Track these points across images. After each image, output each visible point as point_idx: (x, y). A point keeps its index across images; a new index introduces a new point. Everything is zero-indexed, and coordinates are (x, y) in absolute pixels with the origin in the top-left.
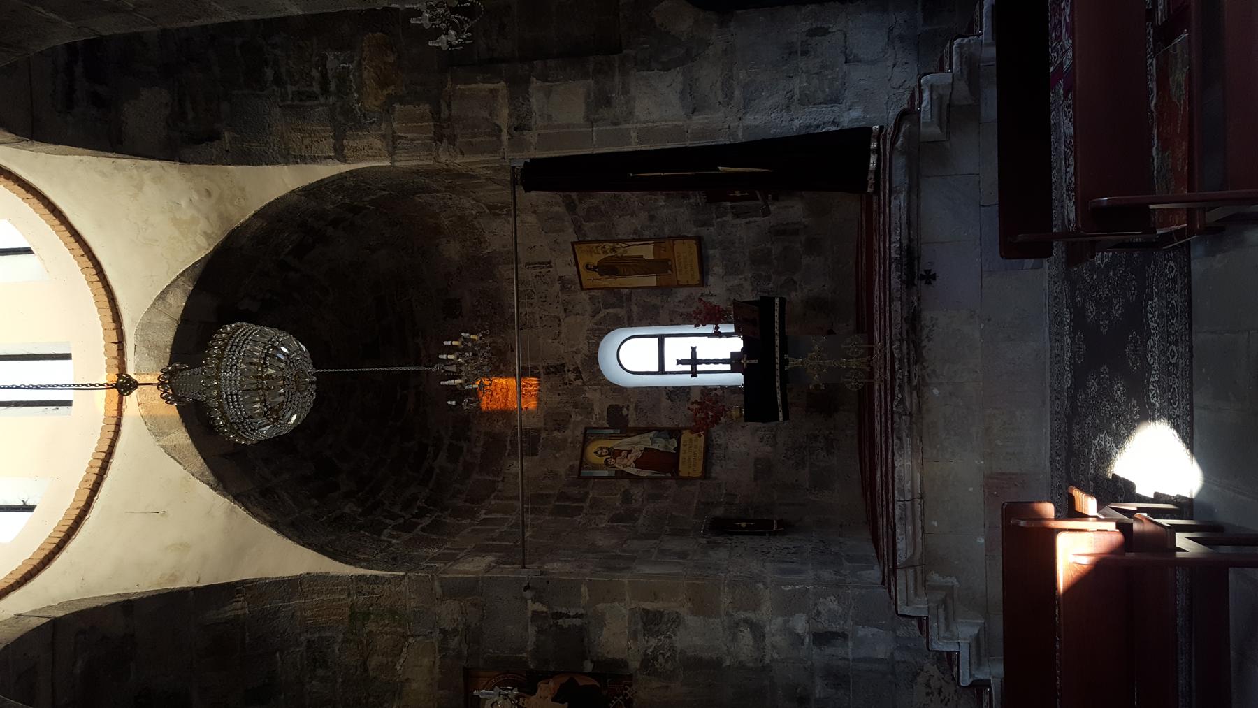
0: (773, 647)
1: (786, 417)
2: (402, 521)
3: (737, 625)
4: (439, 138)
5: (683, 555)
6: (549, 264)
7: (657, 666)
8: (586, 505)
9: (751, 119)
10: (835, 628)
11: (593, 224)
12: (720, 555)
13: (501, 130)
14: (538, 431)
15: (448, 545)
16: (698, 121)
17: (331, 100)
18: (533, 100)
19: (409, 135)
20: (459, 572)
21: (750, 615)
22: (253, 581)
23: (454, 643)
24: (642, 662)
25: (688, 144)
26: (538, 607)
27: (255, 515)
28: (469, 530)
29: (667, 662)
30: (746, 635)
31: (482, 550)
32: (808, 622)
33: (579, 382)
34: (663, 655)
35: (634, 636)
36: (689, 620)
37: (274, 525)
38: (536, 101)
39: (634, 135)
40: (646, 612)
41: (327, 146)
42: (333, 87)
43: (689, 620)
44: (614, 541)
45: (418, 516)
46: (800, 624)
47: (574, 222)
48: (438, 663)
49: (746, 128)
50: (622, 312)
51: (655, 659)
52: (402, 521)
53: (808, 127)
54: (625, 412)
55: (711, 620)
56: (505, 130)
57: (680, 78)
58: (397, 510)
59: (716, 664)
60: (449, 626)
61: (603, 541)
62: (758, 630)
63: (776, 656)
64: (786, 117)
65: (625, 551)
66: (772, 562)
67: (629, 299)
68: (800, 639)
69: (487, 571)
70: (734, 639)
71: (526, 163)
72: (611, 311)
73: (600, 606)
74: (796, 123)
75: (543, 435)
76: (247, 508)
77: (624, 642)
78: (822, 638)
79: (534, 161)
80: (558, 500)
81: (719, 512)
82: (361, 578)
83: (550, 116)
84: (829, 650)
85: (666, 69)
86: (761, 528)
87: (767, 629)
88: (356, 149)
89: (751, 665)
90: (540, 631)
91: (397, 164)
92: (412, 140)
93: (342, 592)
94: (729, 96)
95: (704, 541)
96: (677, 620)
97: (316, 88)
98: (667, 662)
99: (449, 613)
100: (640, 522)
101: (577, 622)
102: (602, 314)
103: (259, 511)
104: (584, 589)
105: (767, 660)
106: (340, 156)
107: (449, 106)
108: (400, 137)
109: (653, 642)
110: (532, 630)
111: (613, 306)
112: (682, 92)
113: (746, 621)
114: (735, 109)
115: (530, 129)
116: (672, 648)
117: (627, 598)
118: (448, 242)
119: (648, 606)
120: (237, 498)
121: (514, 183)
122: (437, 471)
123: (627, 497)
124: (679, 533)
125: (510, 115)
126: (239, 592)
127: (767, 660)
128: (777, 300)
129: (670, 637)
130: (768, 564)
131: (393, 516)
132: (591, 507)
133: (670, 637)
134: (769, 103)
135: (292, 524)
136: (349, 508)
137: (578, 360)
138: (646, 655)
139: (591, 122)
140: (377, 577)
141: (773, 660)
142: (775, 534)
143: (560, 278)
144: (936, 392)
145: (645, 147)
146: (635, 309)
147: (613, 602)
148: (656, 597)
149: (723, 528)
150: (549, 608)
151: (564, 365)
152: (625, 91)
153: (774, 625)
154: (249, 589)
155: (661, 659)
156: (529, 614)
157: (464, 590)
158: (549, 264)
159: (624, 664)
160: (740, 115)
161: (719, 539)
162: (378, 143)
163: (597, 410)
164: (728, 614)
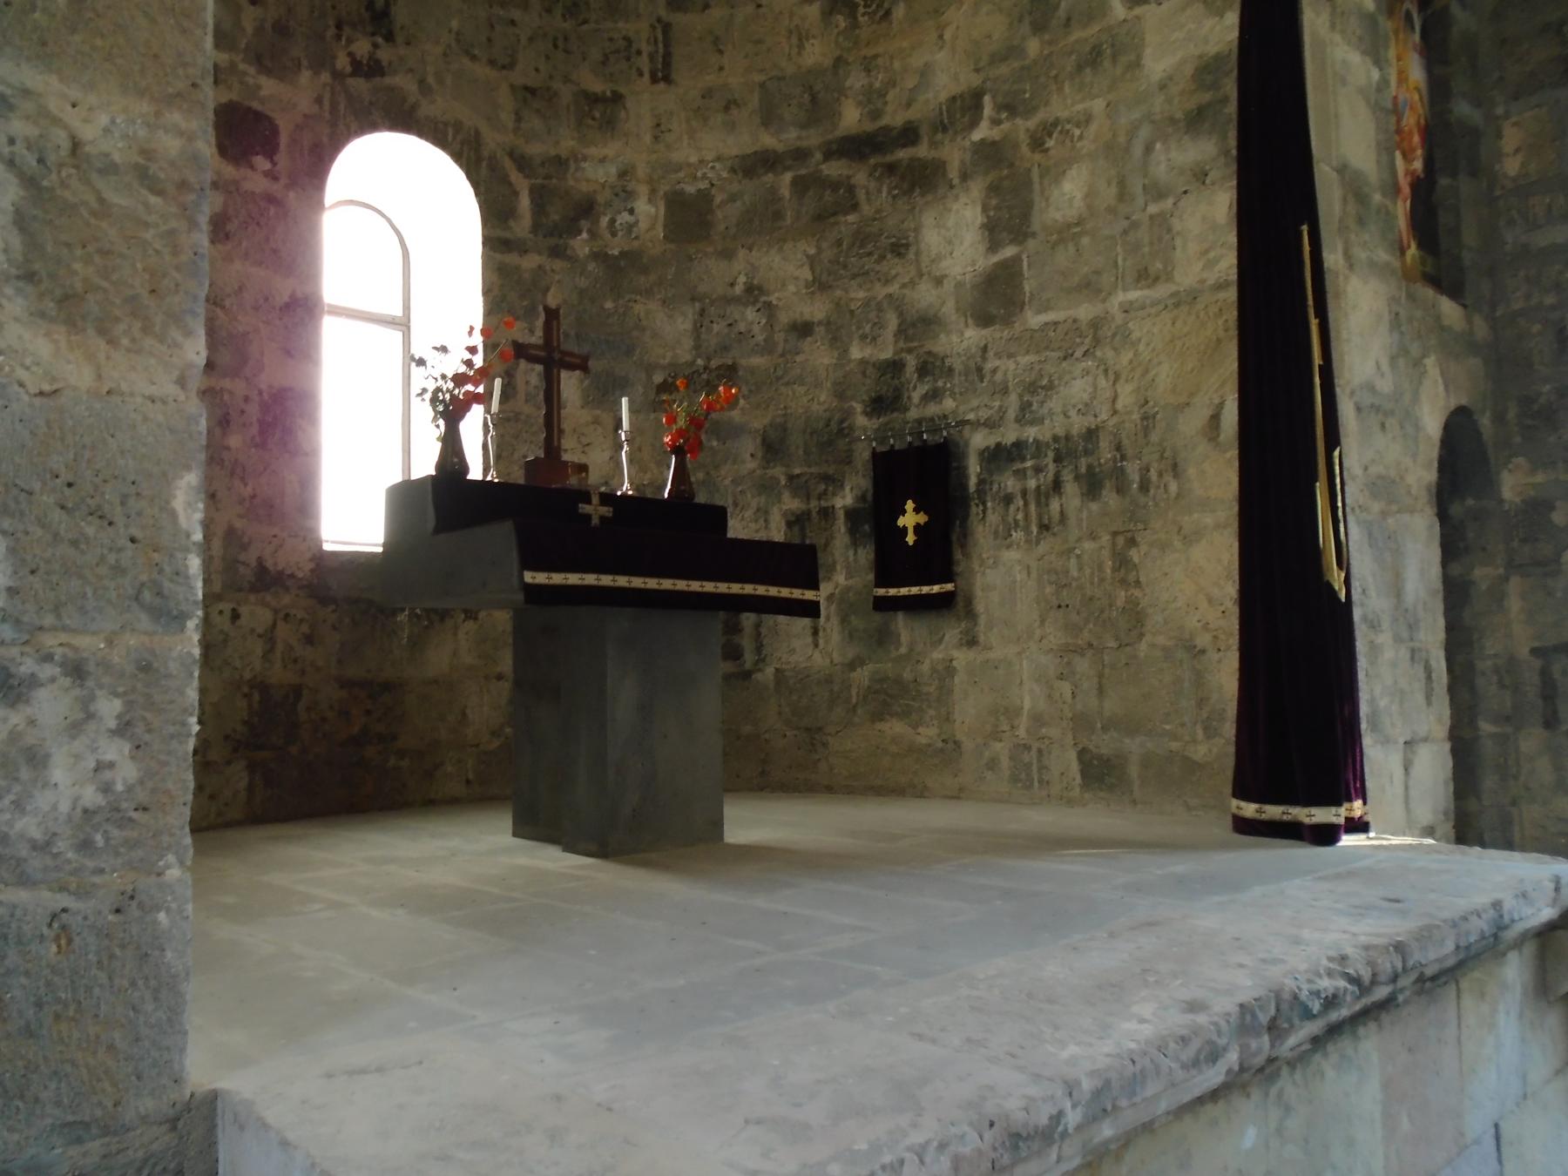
6: (663, 74)
33: (342, 62)
50: (522, 226)
54: (262, 163)
67: (556, 252)
72: (525, 202)
102: (515, 177)
111: (539, 207)
128: (809, 595)
137: (401, 81)
143: (617, 98)
144: (1250, 1137)
146: (530, 262)
151: (390, 38)
158: (663, 74)
163: (269, 86)
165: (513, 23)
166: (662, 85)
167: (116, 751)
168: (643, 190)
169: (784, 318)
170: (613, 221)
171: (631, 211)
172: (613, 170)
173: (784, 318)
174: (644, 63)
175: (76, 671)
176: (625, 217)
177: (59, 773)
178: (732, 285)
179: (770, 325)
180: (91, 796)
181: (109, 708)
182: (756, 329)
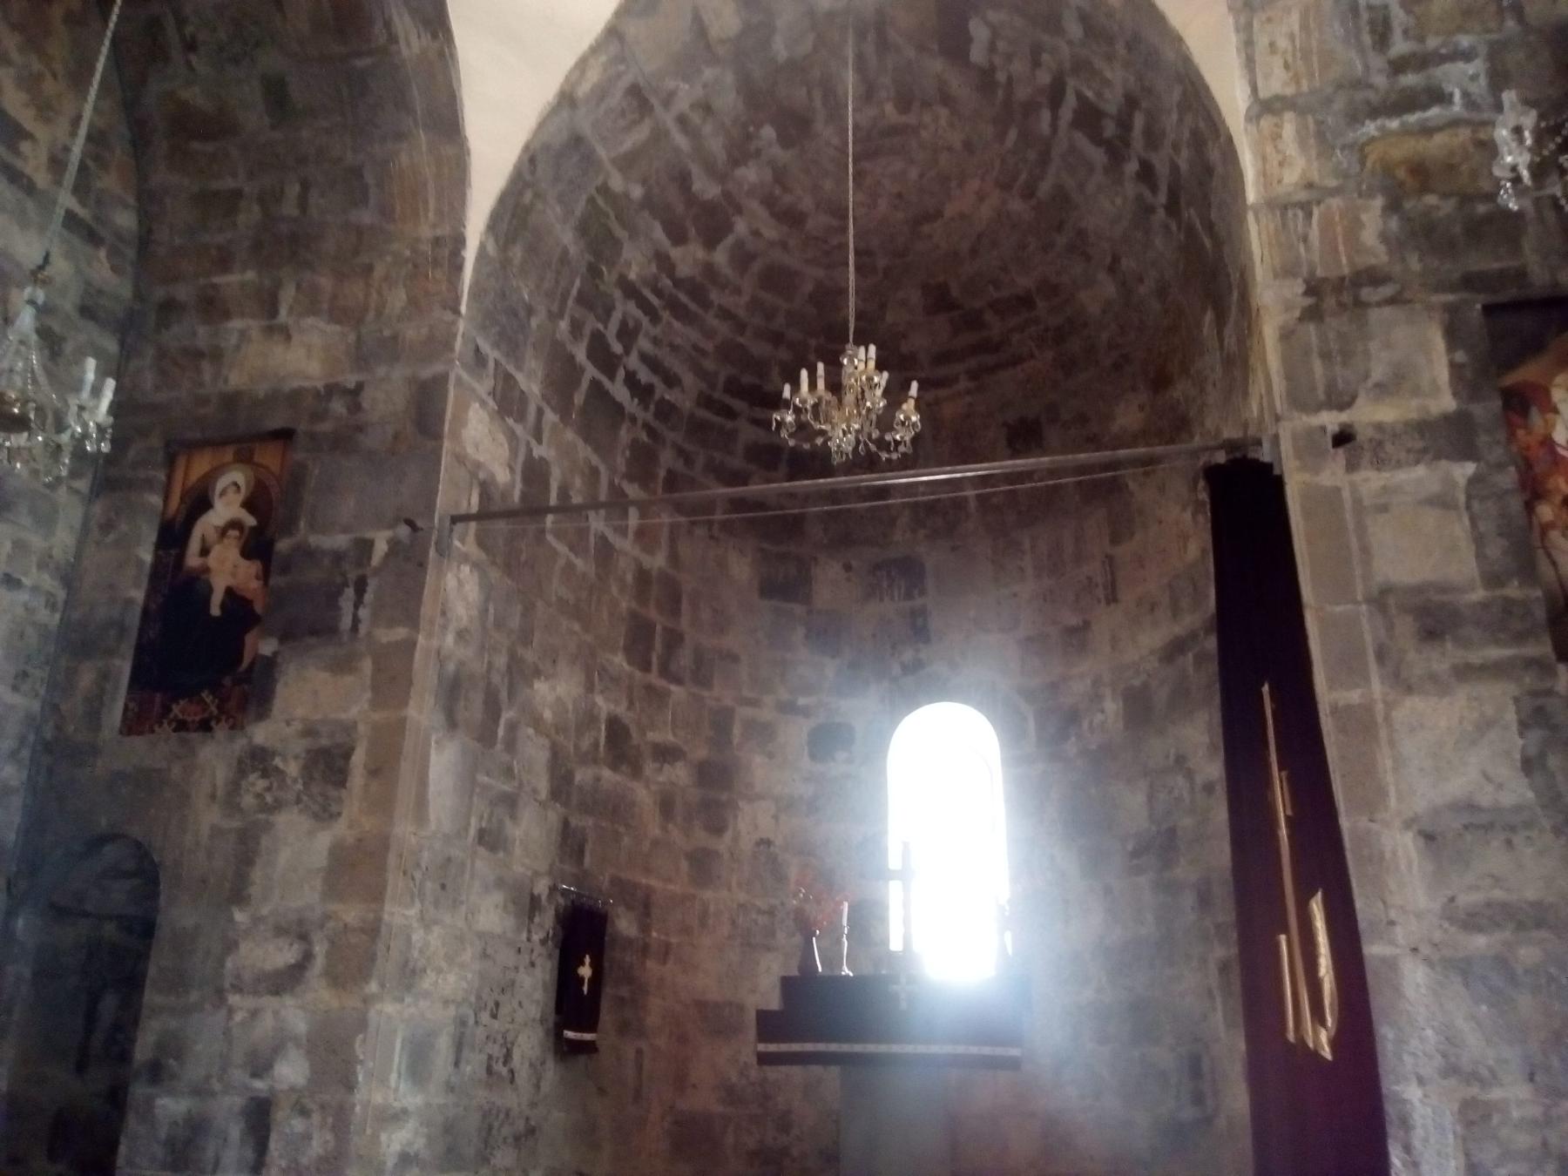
0: (255, 1013)
1: (764, 1059)
2: (617, 348)
3: (304, 937)
4: (1313, 289)
5: (490, 839)
6: (1112, 598)
7: (252, 777)
8: (654, 678)
9: (1415, 979)
10: (275, 1145)
11: (1191, 669)
12: (492, 915)
13: (1343, 406)
14: (807, 600)
15: (550, 417)
16: (1402, 845)
17: (1380, 80)
18: (1420, 471)
19: (1315, 234)
20: (462, 408)
21: (319, 962)
22: (453, 56)
23: (338, 407)
24: (263, 750)
25: (1345, 823)
26: (381, 548)
27: (582, 64)
28: (595, 460)
29: (259, 796)
30: (283, 955)
31: (535, 473)
32: (292, 1089)
34: (269, 789)
35: (310, 731)
36: (324, 840)
37: (566, 99)
38: (1419, 477)
39: (1354, 696)
40: (347, 755)
41: (1276, 83)
42: (1410, 79)
43: (324, 840)
44: (548, 715)
45: (631, 380)
46: (291, 1071)
47: (1194, 635)
48: (306, 384)
49: (1391, 964)
51: (265, 774)
52: (617, 348)
53: (1406, 1124)
55: (318, 883)
56: (1344, 417)
57: (1508, 799)
58: (644, 343)
59: (238, 895)
60: (366, 400)
61: (554, 692)
62: (287, 980)
63: (239, 1017)
64: (1428, 1070)
65: (512, 727)
66: (462, 1023)
68: (261, 1066)
69: (460, 459)
70: (280, 931)
71: (1269, 466)
73: (367, 665)
74: (1413, 1093)
75: (798, 609)
76: (595, 50)
77: (300, 712)
78: (259, 1116)
79: (1278, 484)
80: (665, 629)
81: (624, 924)
82: (460, 241)
83: (1384, 509)
84: (235, 1131)
85: (1529, 765)
86: (574, 1007)
87: (288, 1000)
88: (1276, 137)
89: (229, 964)
90: (338, 557)
91: (1250, 217)
92: (1305, 239)
93: (439, 212)
94: (1472, 921)
95: (542, 887)
96: (326, 815)
97: (1400, 46)
98: (259, 796)
99: (387, 395)
100: (607, 773)
101: (346, 622)
103: (594, 76)
104: (401, 633)
105: (234, 999)
106: (1265, 108)
107: (1392, 301)
108: (1309, 215)
109: (293, 769)
110: (340, 541)
112: (1471, 807)
113: (308, 957)
114: (1437, 936)
115: (1351, 467)
116: (278, 806)
117: (377, 716)
118: (1141, 408)
119: (359, 758)
120: (613, 32)
121: (1230, 446)
122: (729, 425)
123: (666, 754)
124: (570, 843)
125: (1379, 427)
126: (435, 36)
127: (234, 999)
129: (298, 801)
130: (452, 1011)
131: (627, 334)
132: (649, 688)
133: (298, 801)
134: (1461, 1023)
135: (577, 141)
136: (635, 262)
138: (274, 754)
139: (1381, 599)
140: (458, 268)
141: (231, 1011)
142: (558, 1035)
143: (1086, 625)
145: (1327, 724)
147: (375, 688)
148: (374, 772)
149: (580, 932)
150: (377, 571)
152: (1465, 672)
153: (292, 1014)
154: (441, 55)
155: (261, 784)
156: (368, 535)
157: (426, 413)
158: (1112, 598)
159: (263, 713)
160: (1425, 950)
161: (547, 920)
162: (1292, 176)
164: (327, 917)
165: (1015, 595)
166: (1113, 606)
167: (329, 1137)
168: (1108, 692)
169: (1199, 780)
170: (1091, 723)
171: (1103, 711)
172: (1089, 682)
173: (1199, 780)
174: (1100, 592)
175: (323, 1107)
176: (1099, 717)
177: (314, 1143)
178: (1167, 757)
179: (1192, 789)
180: (321, 1151)
181: (330, 1120)
182: (1185, 794)
